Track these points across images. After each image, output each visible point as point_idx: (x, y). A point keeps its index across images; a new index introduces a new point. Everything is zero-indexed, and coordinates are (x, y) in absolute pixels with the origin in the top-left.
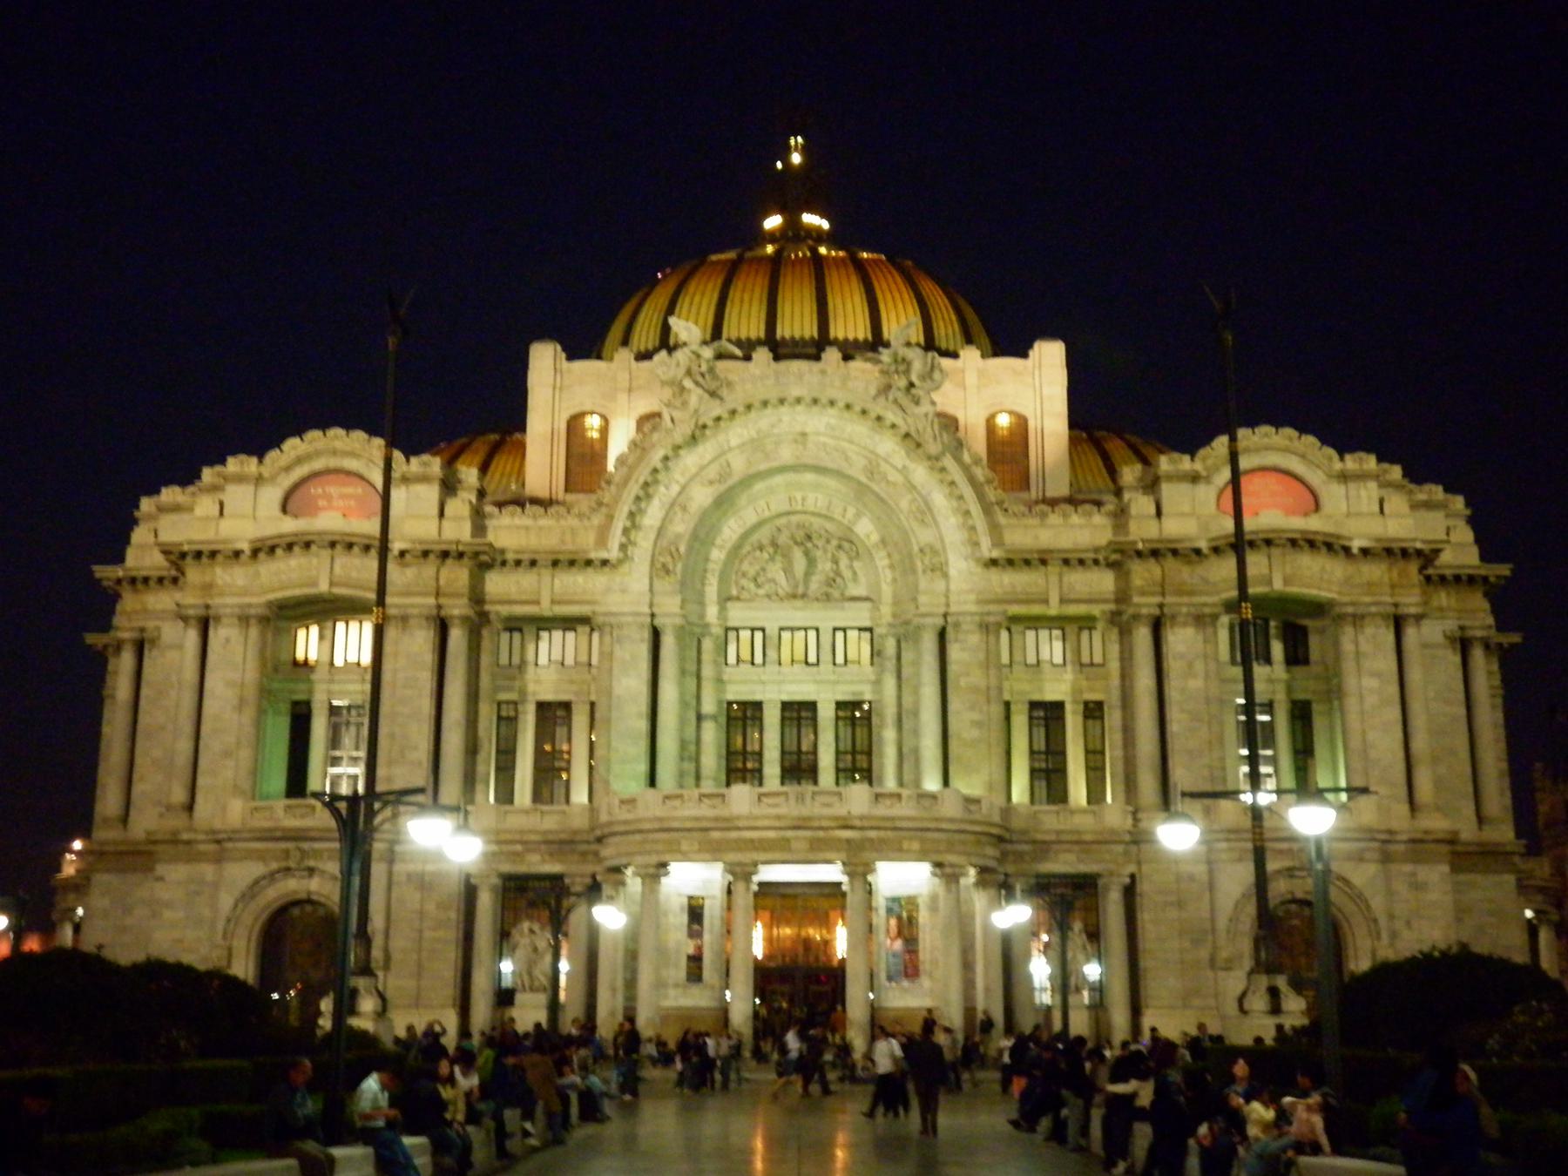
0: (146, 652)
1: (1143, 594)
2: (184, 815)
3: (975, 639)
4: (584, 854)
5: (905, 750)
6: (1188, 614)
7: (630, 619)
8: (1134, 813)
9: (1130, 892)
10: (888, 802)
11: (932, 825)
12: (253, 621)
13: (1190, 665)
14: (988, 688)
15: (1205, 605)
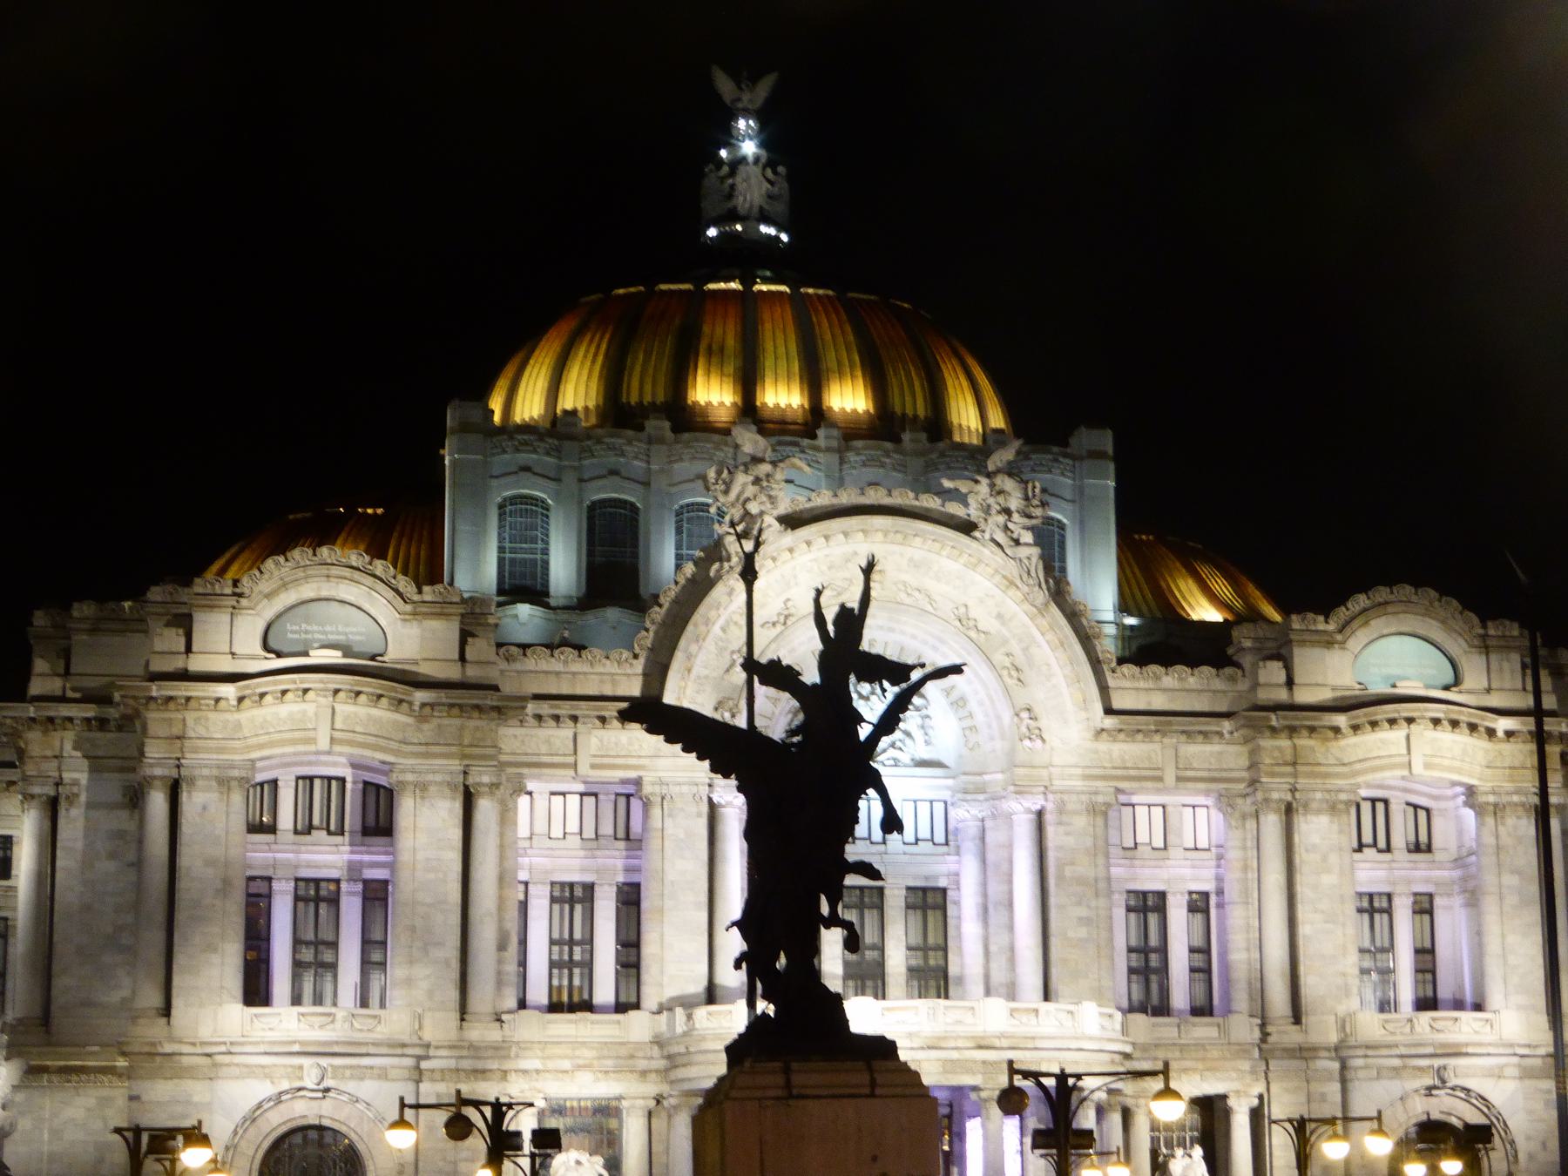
0: (62, 813)
1: (1273, 775)
2: (164, 1020)
3: (1081, 822)
4: (644, 1073)
5: (993, 948)
6: (1321, 801)
7: (685, 789)
8: (1263, 1026)
9: (1257, 1115)
10: (1024, 1019)
11: (1074, 1045)
12: (234, 784)
13: (1325, 859)
14: (1096, 880)
15: (1340, 791)
